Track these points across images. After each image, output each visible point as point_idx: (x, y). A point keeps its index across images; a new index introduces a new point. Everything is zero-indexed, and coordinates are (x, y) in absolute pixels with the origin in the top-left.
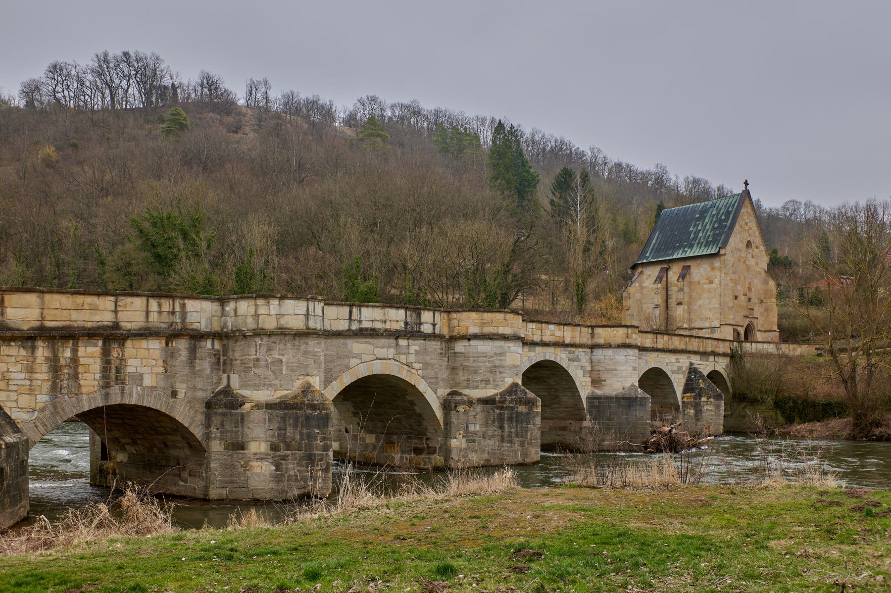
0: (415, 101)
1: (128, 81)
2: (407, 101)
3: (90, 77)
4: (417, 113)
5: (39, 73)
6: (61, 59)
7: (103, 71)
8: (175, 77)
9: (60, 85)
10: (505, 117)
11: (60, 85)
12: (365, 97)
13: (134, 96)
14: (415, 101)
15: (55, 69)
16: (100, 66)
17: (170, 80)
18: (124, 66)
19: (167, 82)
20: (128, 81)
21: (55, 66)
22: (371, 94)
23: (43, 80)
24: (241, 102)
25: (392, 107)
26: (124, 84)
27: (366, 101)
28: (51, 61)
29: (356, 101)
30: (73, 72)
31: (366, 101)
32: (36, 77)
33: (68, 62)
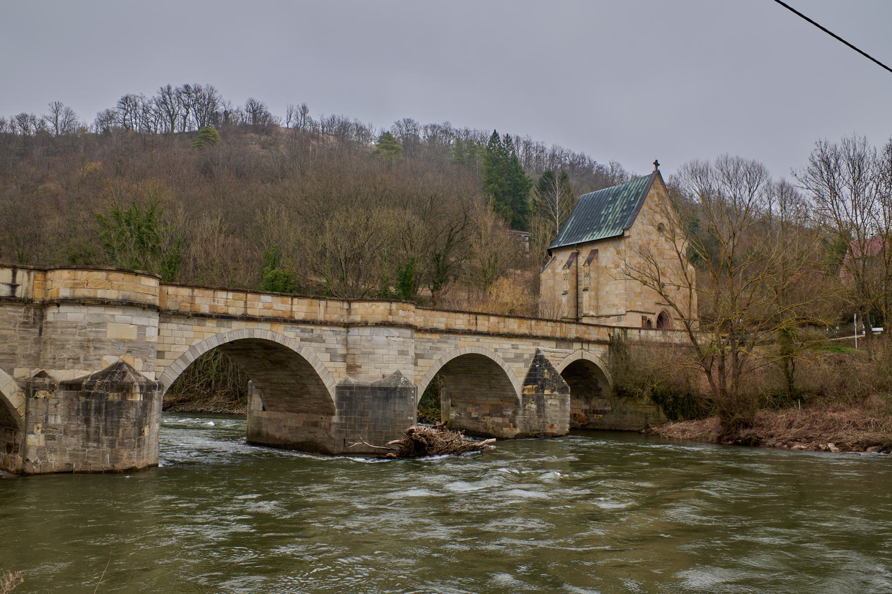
0: (447, 123)
1: (187, 110)
2: (440, 122)
3: (154, 106)
4: (446, 132)
5: (113, 105)
8: (227, 105)
9: (129, 114)
10: (527, 135)
11: (129, 114)
15: (126, 100)
16: (164, 97)
17: (223, 107)
19: (221, 109)
20: (187, 110)
21: (126, 98)
24: (283, 124)
25: (426, 128)
26: (184, 111)
27: (402, 123)
28: (124, 95)
29: (394, 124)
30: (140, 104)
31: (402, 123)
32: (110, 108)
33: (136, 94)
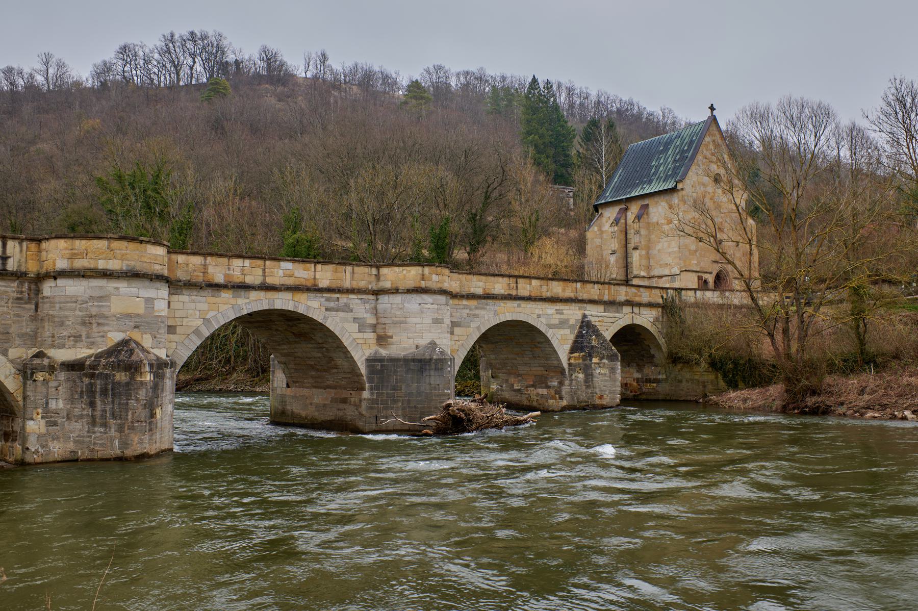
0: (481, 69)
1: (194, 59)
2: (473, 68)
3: (156, 56)
4: (480, 79)
5: (110, 55)
6: (130, 40)
7: (168, 49)
8: (237, 53)
9: (128, 65)
10: (570, 80)
11: (128, 65)
12: (431, 67)
14: (481, 69)
15: (124, 49)
17: (233, 56)
18: (189, 45)
19: (231, 58)
20: (194, 59)
21: (125, 47)
22: (437, 63)
23: (114, 61)
25: (458, 75)
27: (432, 70)
28: (122, 43)
29: (423, 71)
30: (141, 53)
31: (432, 70)
32: (107, 59)
33: (135, 43)
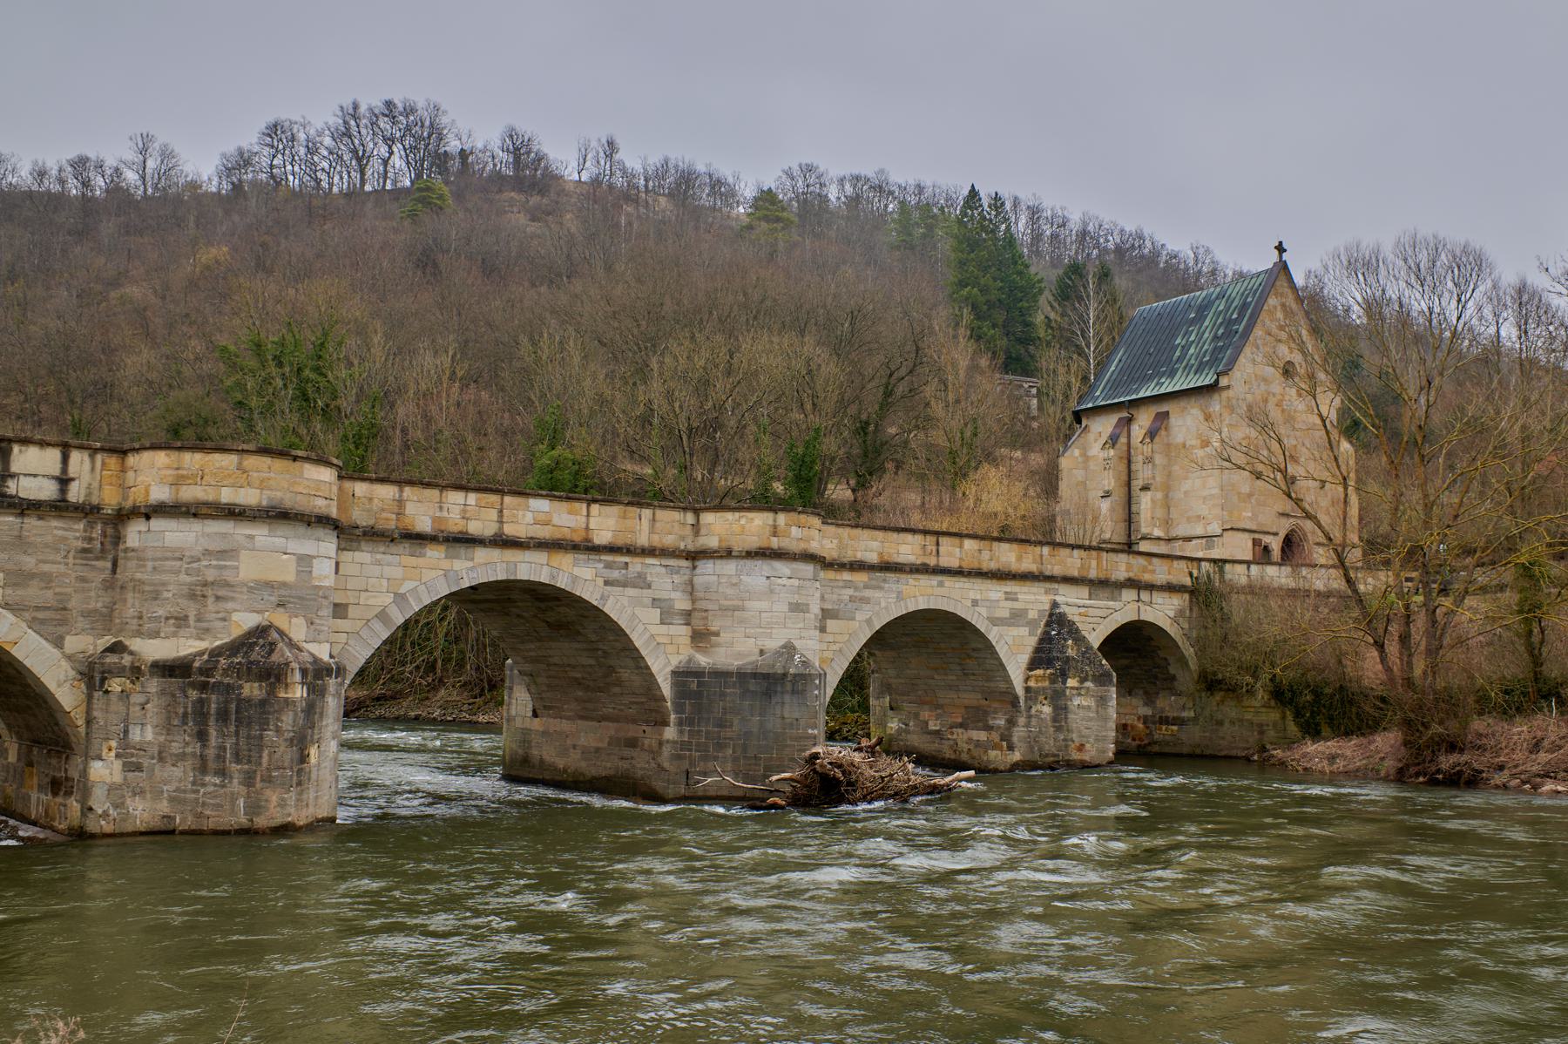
0: (882, 171)
1: (390, 147)
2: (868, 171)
3: (328, 141)
4: (879, 189)
5: (250, 139)
6: (283, 114)
7: (348, 129)
8: (464, 138)
9: (280, 156)
10: (1034, 195)
11: (280, 156)
13: (401, 172)
14: (882, 171)
15: (274, 129)
16: (345, 122)
17: (458, 143)
18: (384, 123)
19: (453, 146)
20: (390, 147)
21: (275, 126)
22: (806, 160)
23: (256, 149)
25: (841, 181)
26: (384, 150)
27: (796, 172)
28: (271, 119)
29: (781, 174)
30: (302, 136)
31: (796, 172)
32: (245, 145)
33: (294, 119)
